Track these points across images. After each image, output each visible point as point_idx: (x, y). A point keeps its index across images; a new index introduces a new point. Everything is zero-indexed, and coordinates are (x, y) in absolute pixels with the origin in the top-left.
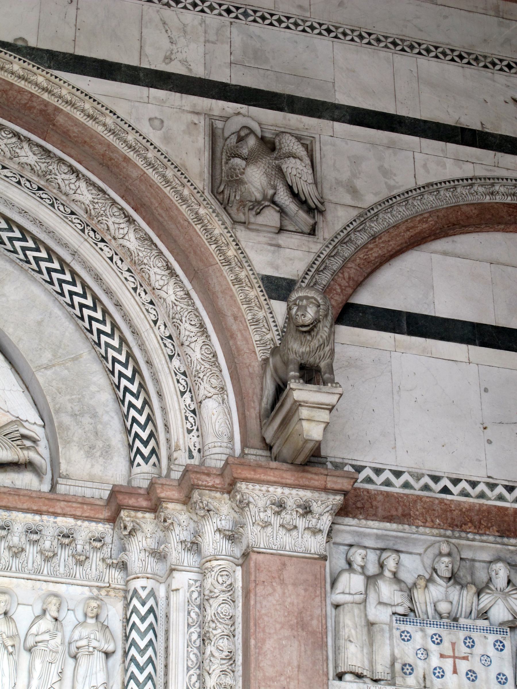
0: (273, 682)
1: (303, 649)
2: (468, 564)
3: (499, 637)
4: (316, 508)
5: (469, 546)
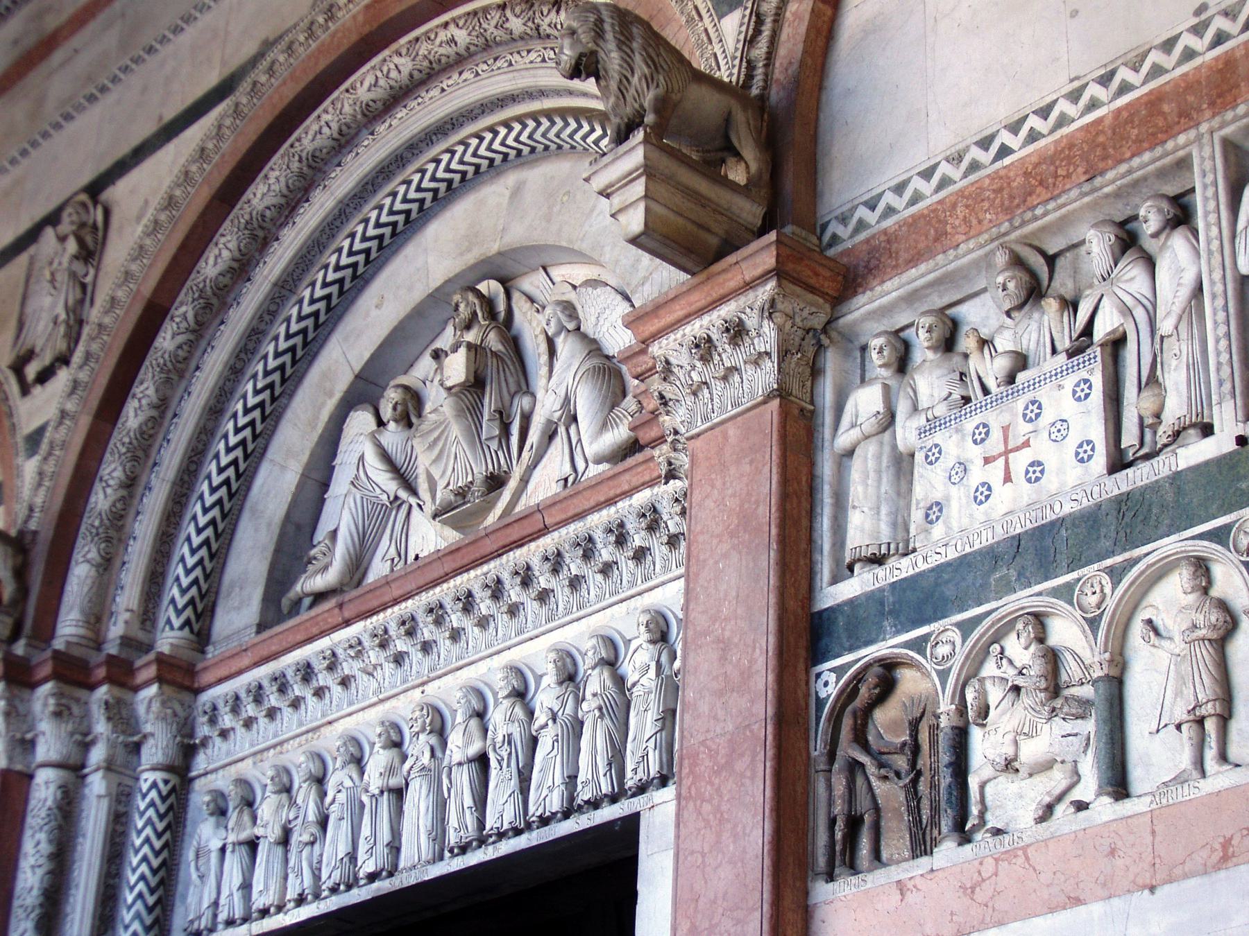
4: (751, 321)
5: (1043, 229)
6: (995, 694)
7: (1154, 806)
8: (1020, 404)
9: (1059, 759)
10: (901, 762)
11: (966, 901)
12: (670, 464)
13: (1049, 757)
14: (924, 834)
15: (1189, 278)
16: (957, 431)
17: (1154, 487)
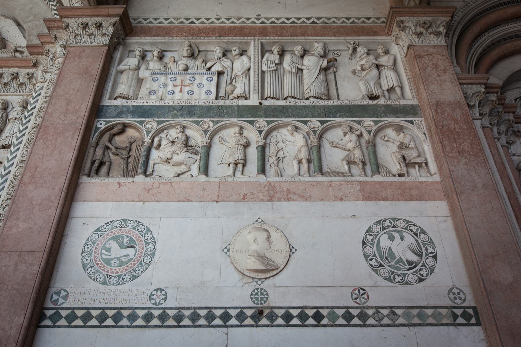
0: (61, 97)
1: (83, 82)
2: (204, 53)
3: (211, 76)
5: (202, 42)
6: (164, 142)
7: (221, 181)
8: (188, 77)
9: (185, 163)
10: (124, 153)
11: (146, 193)
12: (36, 61)
13: (182, 162)
14: (128, 173)
15: (247, 66)
16: (165, 76)
17: (231, 106)
